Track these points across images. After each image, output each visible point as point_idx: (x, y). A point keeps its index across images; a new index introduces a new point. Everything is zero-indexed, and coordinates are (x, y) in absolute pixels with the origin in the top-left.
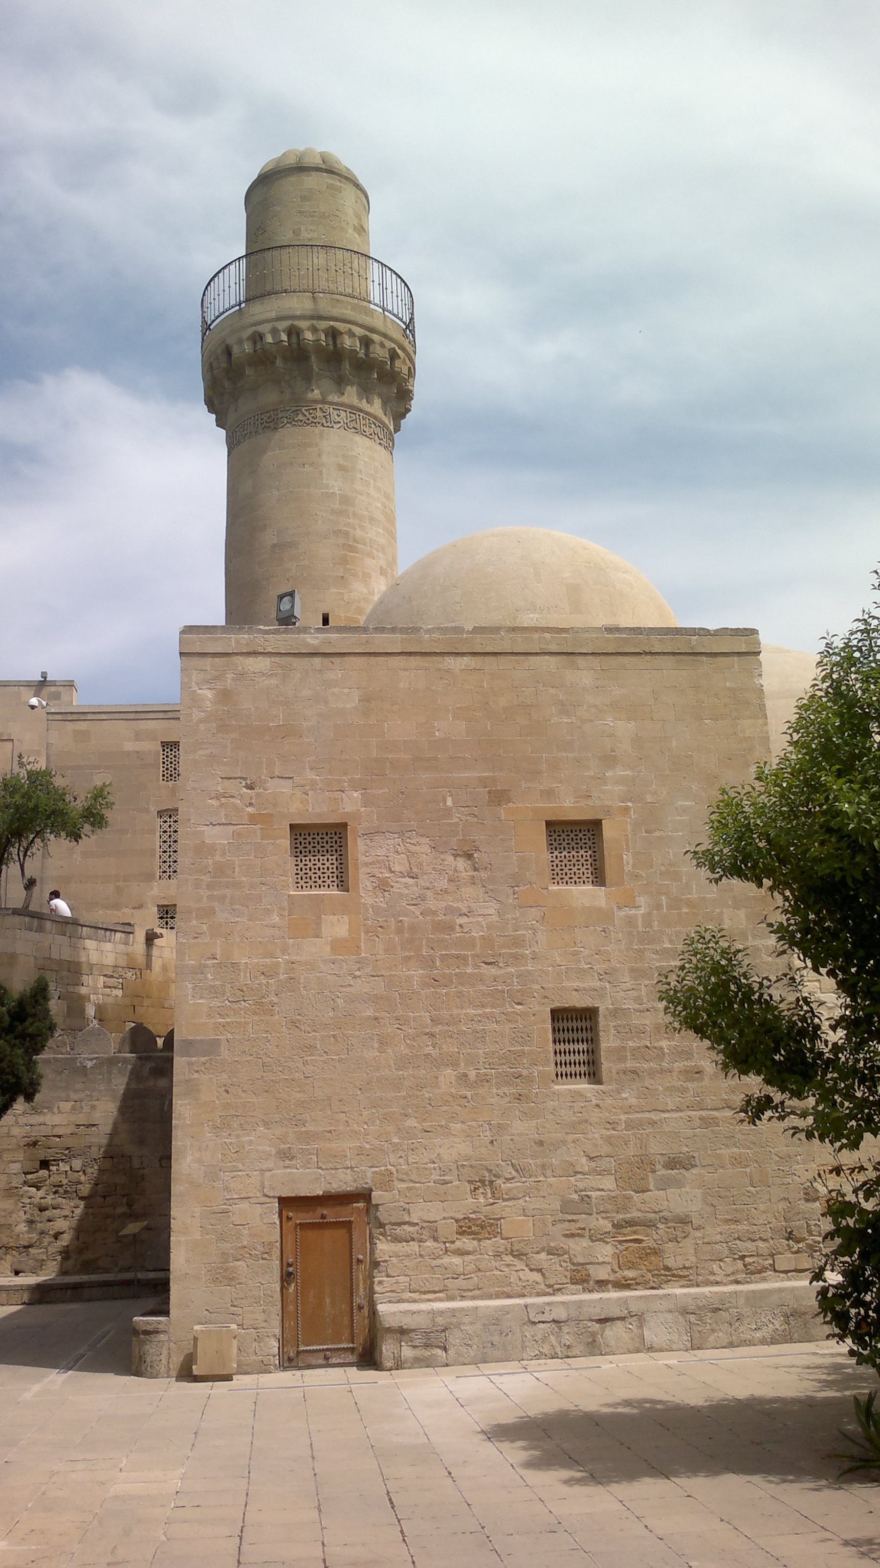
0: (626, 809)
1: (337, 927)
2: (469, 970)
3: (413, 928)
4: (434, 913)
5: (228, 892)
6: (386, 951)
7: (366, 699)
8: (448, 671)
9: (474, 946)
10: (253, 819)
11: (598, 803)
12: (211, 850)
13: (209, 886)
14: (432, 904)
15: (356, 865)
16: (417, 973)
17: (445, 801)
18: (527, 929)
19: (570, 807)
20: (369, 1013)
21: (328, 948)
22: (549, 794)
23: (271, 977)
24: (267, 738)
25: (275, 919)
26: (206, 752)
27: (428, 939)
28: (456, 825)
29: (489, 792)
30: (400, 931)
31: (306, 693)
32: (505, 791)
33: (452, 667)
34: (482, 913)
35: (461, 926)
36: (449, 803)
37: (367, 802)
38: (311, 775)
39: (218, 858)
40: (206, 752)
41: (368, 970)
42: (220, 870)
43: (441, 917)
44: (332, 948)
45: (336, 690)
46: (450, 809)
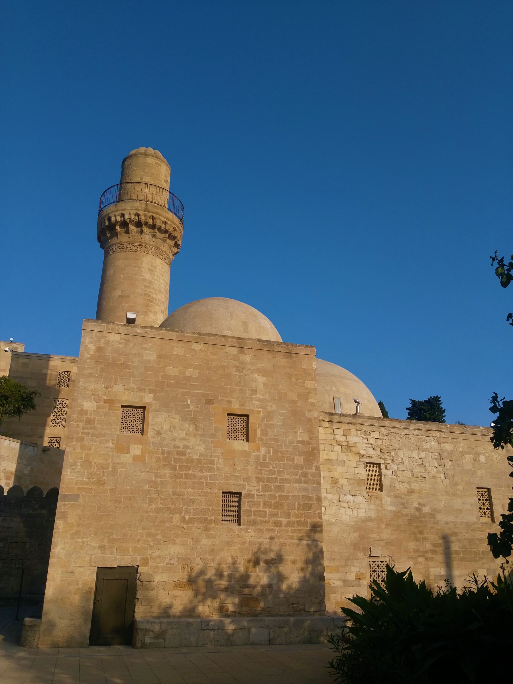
0: (260, 411)
1: (136, 450)
2: (190, 472)
3: (169, 453)
4: (178, 447)
5: (91, 431)
6: (156, 462)
7: (159, 357)
8: (194, 350)
9: (193, 462)
10: (106, 401)
11: (248, 408)
12: (86, 412)
13: (83, 428)
14: (177, 443)
15: (148, 424)
16: (167, 472)
17: (187, 401)
18: (215, 457)
19: (236, 408)
20: (147, 488)
21: (132, 459)
22: (229, 402)
23: (106, 469)
24: (116, 368)
25: (110, 444)
26: (88, 371)
27: (175, 459)
28: (191, 411)
29: (206, 400)
30: (163, 453)
31: (134, 352)
32: (212, 399)
33: (196, 348)
34: (197, 448)
35: (189, 453)
36: (189, 403)
37: (155, 398)
38: (132, 385)
39: (88, 416)
40: (88, 371)
41: (148, 469)
42: (89, 421)
43: (181, 449)
44: (134, 459)
45: (147, 352)
46: (189, 405)
